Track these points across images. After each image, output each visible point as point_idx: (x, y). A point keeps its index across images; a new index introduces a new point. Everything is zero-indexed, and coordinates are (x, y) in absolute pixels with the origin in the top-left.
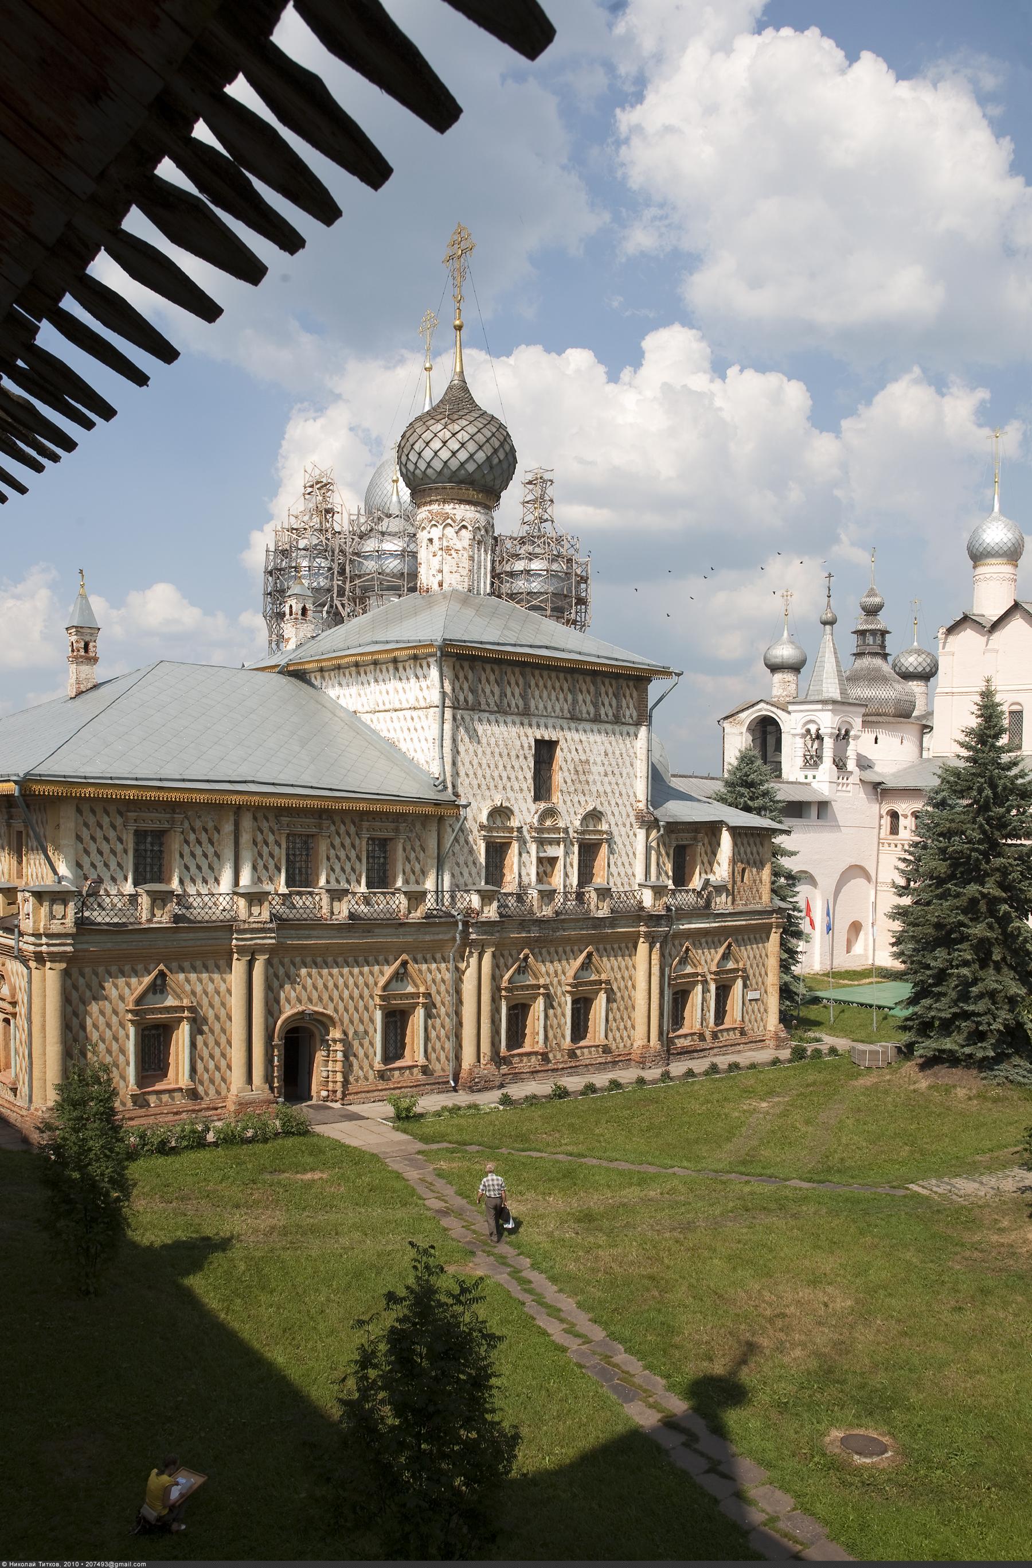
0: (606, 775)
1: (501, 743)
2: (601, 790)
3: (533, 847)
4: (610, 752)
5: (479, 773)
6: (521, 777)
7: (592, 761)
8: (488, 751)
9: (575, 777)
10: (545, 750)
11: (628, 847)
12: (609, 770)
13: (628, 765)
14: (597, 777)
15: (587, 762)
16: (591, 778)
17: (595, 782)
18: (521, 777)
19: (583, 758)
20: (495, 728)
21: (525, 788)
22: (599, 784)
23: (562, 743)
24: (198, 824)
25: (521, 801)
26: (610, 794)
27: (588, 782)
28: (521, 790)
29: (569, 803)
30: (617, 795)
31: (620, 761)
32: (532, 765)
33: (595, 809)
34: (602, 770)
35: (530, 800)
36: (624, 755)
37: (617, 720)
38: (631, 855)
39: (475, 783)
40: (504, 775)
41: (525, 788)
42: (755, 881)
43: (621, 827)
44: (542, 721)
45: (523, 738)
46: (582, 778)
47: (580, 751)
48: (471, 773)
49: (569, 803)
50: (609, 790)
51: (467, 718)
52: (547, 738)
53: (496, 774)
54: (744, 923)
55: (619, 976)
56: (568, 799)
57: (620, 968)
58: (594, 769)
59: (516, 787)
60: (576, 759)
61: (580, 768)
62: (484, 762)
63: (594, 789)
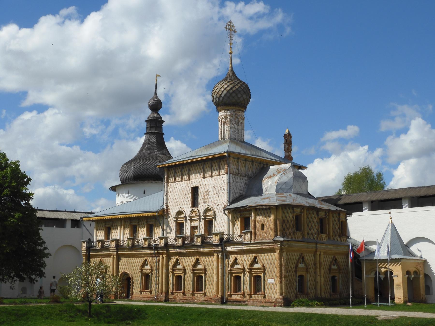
0: (214, 195)
1: (181, 191)
2: (213, 200)
3: (189, 222)
4: (216, 185)
5: (175, 201)
6: (187, 200)
7: (209, 190)
8: (177, 194)
9: (203, 197)
10: (195, 191)
11: (223, 220)
12: (215, 194)
13: (222, 189)
14: (211, 196)
15: (207, 191)
16: (209, 198)
17: (210, 198)
18: (187, 200)
19: (206, 190)
20: (179, 186)
21: (188, 203)
22: (212, 198)
23: (199, 187)
24: (115, 224)
25: (187, 208)
26: (216, 201)
27: (208, 198)
28: (187, 204)
29: (202, 207)
30: (219, 201)
31: (219, 189)
32: (190, 195)
33: (208, 207)
34: (213, 193)
35: (190, 207)
36: (221, 186)
37: (219, 175)
38: (224, 223)
39: (174, 204)
40: (182, 201)
41: (188, 203)
42: (268, 229)
43: (220, 213)
44: (193, 181)
45: (187, 188)
46: (206, 197)
47: (205, 188)
48: (173, 201)
49: (202, 207)
50: (215, 200)
51: (172, 185)
52: (194, 186)
53: (180, 201)
54: (259, 247)
55: (210, 268)
56: (201, 205)
57: (211, 265)
58: (210, 193)
59: (186, 204)
60: (204, 191)
61: (205, 194)
62: (176, 198)
63: (210, 200)
